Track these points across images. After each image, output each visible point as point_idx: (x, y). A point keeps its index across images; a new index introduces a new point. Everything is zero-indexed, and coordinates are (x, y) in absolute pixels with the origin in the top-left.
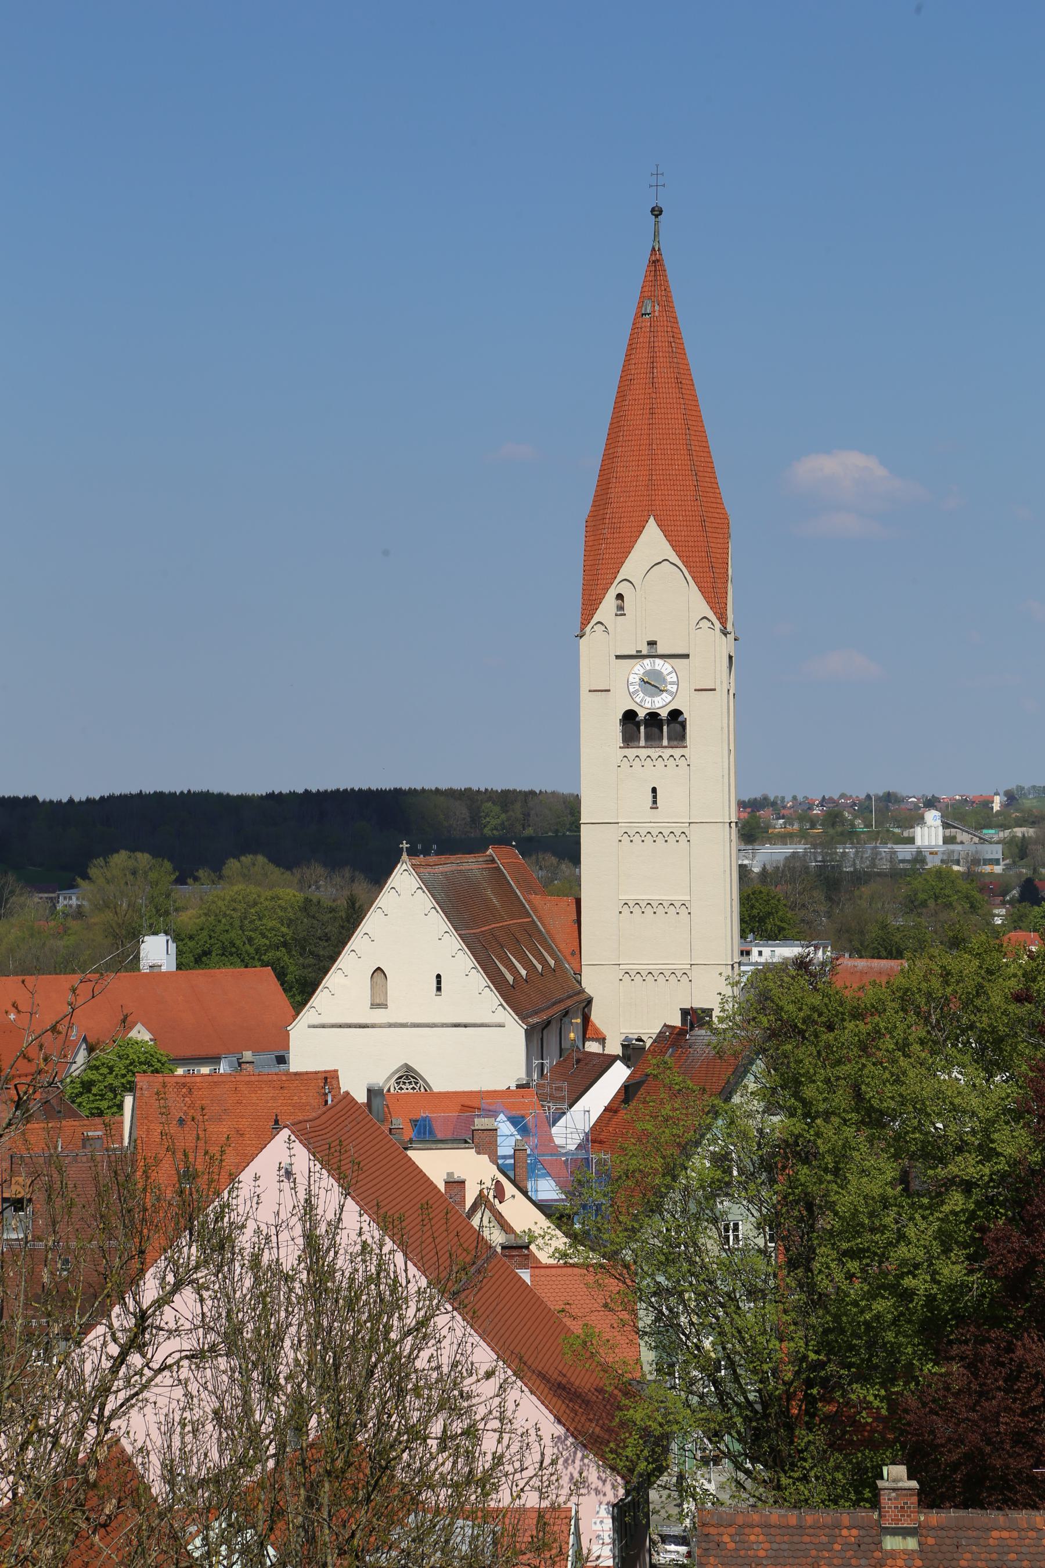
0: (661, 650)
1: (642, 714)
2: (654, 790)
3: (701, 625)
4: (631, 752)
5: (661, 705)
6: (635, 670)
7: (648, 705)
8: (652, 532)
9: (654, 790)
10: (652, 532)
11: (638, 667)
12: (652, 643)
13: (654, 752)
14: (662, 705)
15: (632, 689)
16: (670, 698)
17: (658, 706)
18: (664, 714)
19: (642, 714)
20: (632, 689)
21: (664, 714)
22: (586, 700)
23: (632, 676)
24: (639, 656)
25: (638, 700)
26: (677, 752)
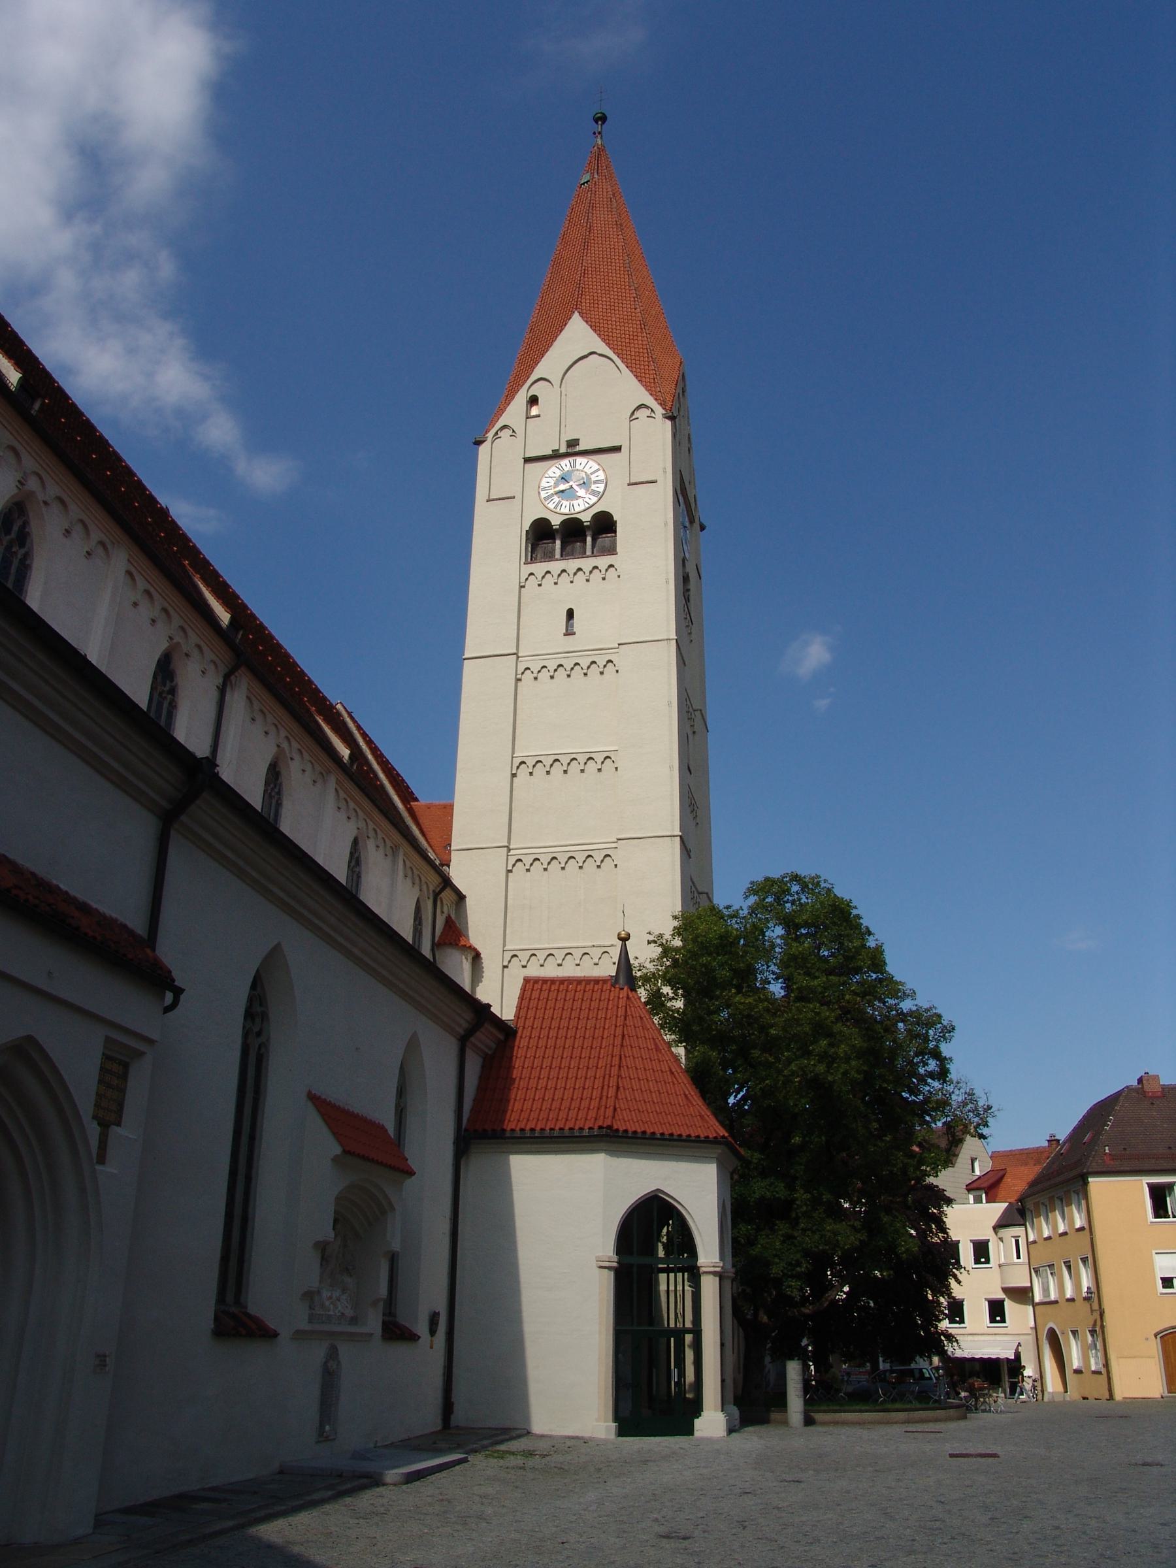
0: (581, 447)
1: (556, 521)
2: (570, 614)
3: (636, 415)
4: (539, 568)
5: (582, 508)
6: (550, 473)
7: (567, 511)
8: (576, 315)
9: (570, 614)
10: (576, 315)
11: (554, 469)
12: (572, 443)
13: (572, 564)
14: (582, 506)
15: (543, 494)
16: (594, 499)
17: (577, 509)
18: (586, 518)
19: (556, 521)
20: (543, 494)
21: (586, 518)
22: (484, 516)
23: (544, 480)
24: (556, 456)
25: (551, 506)
26: (603, 562)
